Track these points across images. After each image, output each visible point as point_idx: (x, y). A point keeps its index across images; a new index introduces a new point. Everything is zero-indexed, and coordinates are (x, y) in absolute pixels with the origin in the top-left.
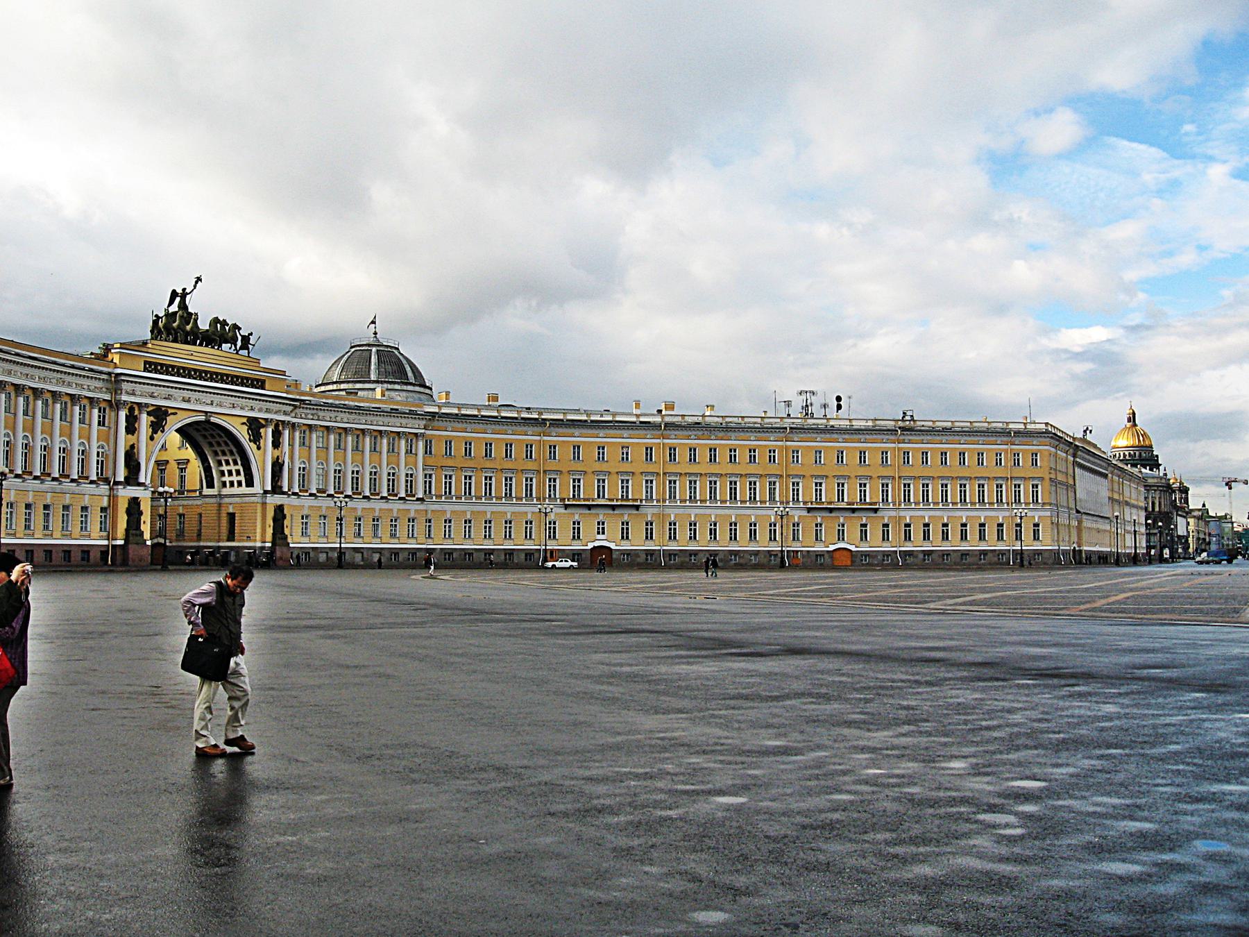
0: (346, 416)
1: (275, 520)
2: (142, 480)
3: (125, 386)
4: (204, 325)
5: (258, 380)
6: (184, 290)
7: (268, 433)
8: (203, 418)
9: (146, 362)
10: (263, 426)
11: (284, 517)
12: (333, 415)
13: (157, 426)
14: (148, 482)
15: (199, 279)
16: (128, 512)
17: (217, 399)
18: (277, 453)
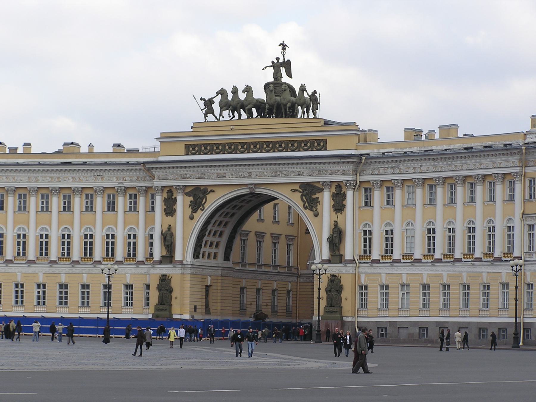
0: (430, 165)
1: (328, 291)
2: (178, 256)
3: (154, 172)
4: (260, 94)
5: (319, 141)
6: (278, 59)
7: (326, 199)
9: (187, 147)
10: (322, 190)
11: (340, 289)
12: (417, 165)
13: (196, 205)
14: (189, 258)
15: (284, 47)
16: (159, 288)
17: (254, 170)
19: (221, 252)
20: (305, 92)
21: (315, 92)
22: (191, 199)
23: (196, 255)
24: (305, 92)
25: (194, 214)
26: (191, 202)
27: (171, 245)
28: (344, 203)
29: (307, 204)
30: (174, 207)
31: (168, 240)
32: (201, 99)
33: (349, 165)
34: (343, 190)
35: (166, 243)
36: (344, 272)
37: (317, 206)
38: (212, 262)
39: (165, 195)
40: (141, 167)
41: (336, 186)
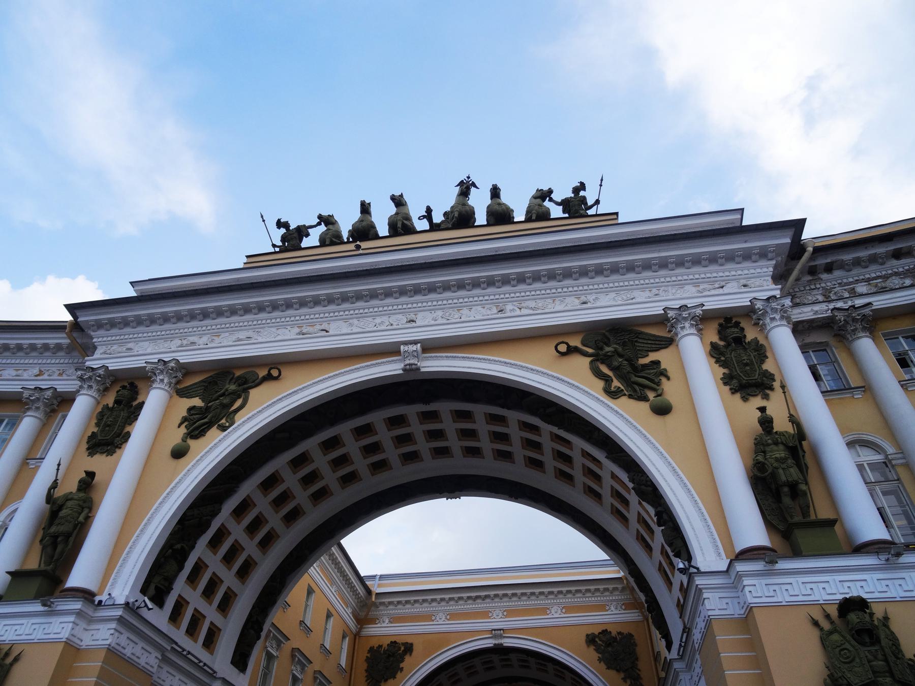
3: (98, 337)
7: (693, 361)
8: (389, 368)
14: (123, 587)
18: (757, 402)
19: (231, 628)
20: (547, 203)
21: (582, 186)
22: (197, 402)
23: (156, 583)
24: (547, 203)
25: (192, 443)
26: (190, 409)
27: (68, 536)
28: (768, 366)
29: (616, 383)
30: (127, 429)
31: (64, 524)
32: (280, 224)
33: (763, 263)
34: (751, 334)
35: (53, 529)
36: (895, 592)
37: (659, 384)
38: (195, 648)
39: (110, 400)
40: (62, 339)
41: (720, 325)
